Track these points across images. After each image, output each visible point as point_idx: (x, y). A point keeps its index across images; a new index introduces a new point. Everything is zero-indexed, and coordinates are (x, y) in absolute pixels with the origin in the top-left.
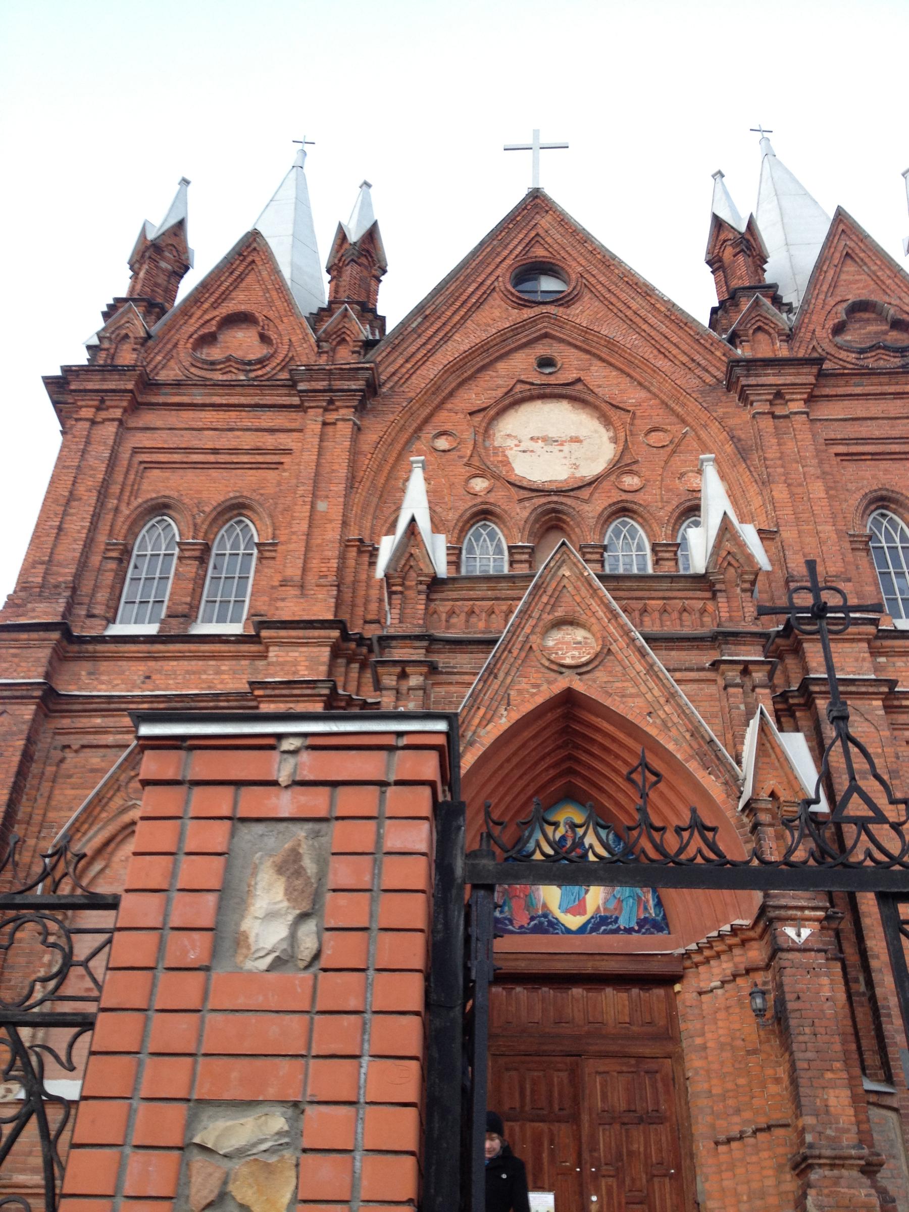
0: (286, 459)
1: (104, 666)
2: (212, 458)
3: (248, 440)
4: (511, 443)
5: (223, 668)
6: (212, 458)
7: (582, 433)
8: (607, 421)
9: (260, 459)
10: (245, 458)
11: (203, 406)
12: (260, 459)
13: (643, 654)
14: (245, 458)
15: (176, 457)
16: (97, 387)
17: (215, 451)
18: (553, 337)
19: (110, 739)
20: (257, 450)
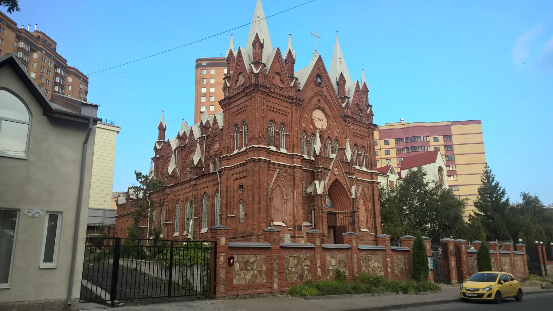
0: (288, 114)
1: (271, 155)
2: (277, 111)
3: (283, 109)
4: (314, 118)
5: (286, 159)
6: (277, 111)
7: (323, 119)
8: (326, 117)
9: (284, 113)
10: (282, 112)
11: (275, 97)
12: (284, 113)
13: (344, 174)
14: (282, 112)
15: (272, 109)
16: (263, 90)
17: (278, 110)
18: (321, 96)
19: (273, 169)
20: (284, 111)
